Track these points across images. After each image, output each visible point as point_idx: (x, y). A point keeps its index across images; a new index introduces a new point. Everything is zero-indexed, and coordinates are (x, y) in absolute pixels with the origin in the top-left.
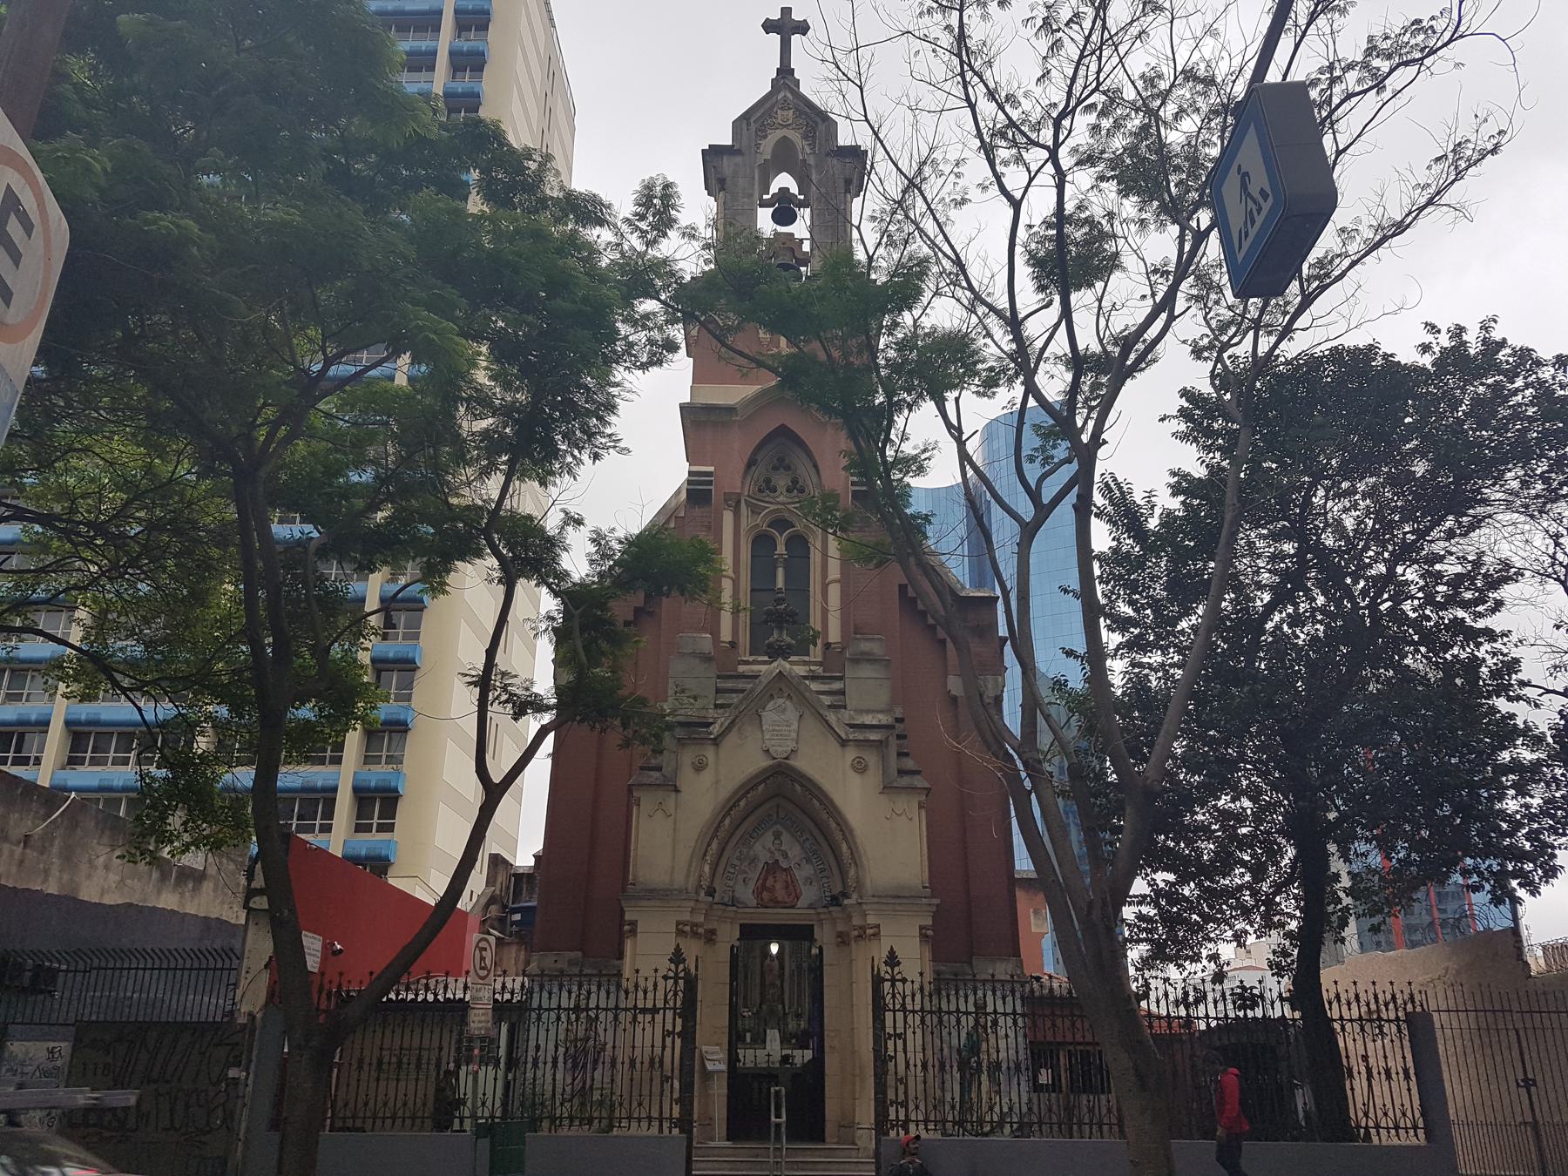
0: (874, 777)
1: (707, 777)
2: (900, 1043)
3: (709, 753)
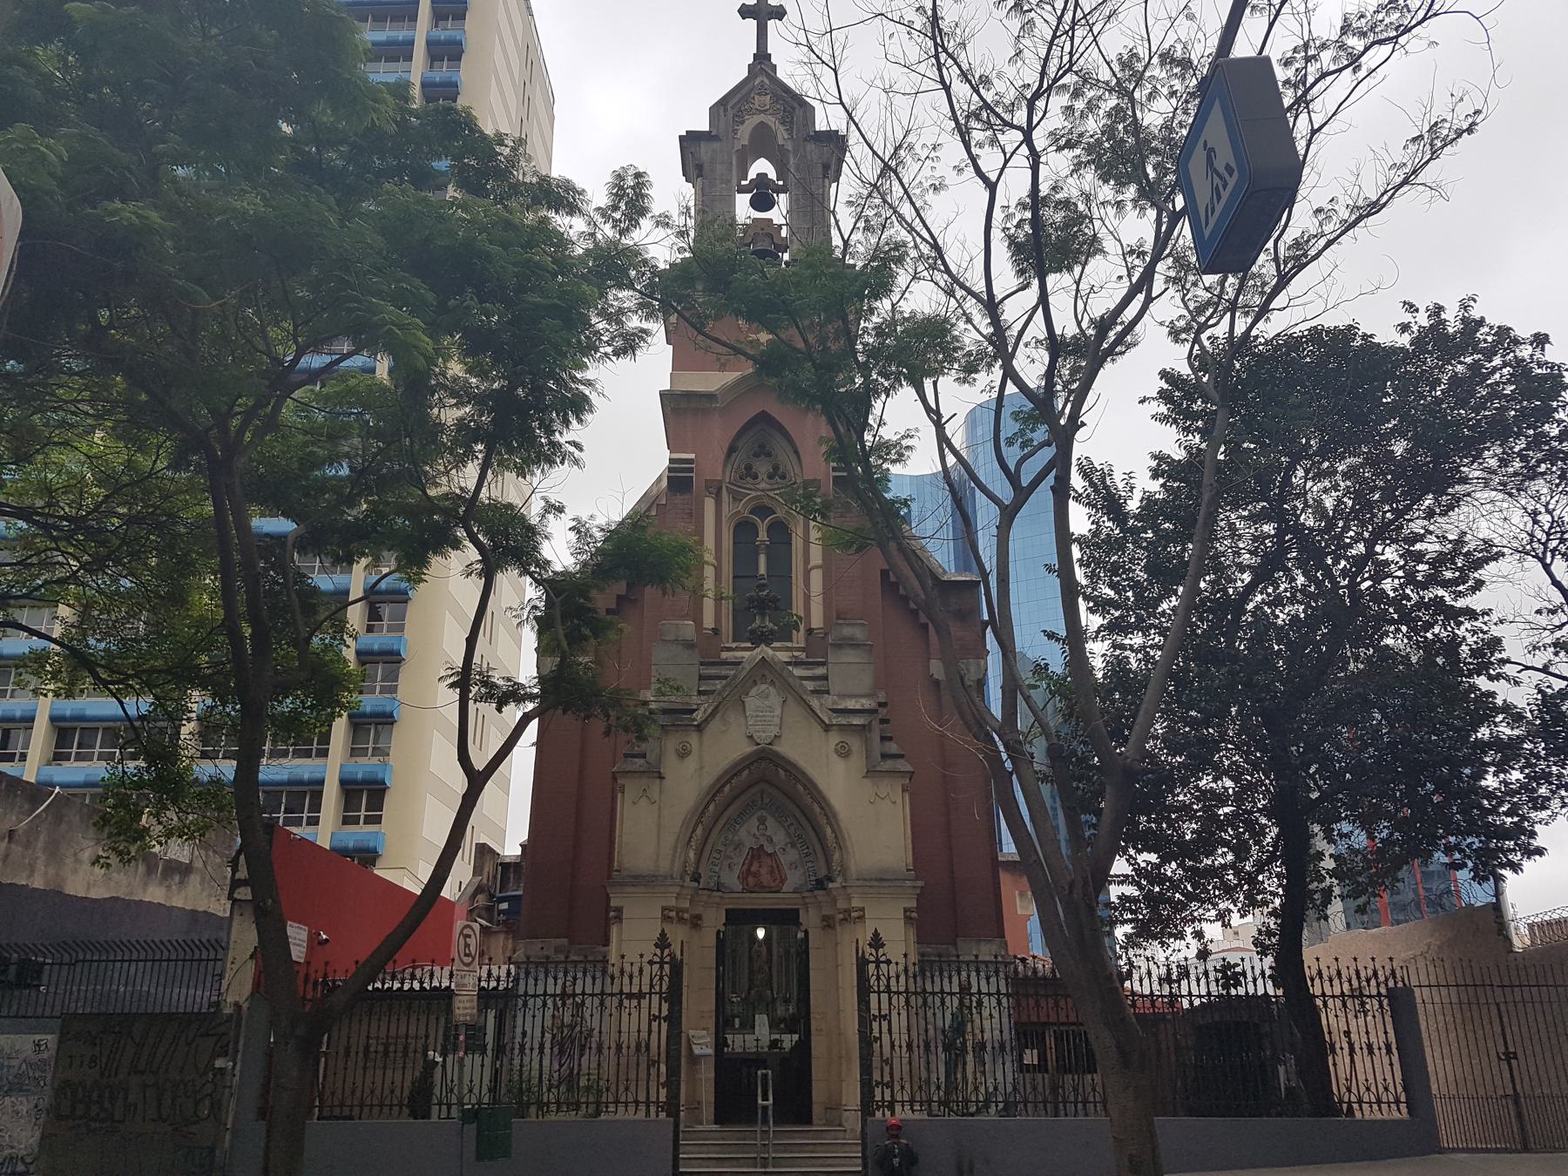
0: (857, 761)
1: (691, 763)
2: (885, 1024)
3: (693, 739)
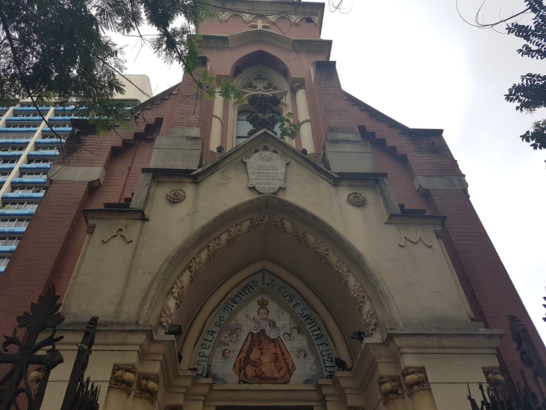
1: (183, 209)
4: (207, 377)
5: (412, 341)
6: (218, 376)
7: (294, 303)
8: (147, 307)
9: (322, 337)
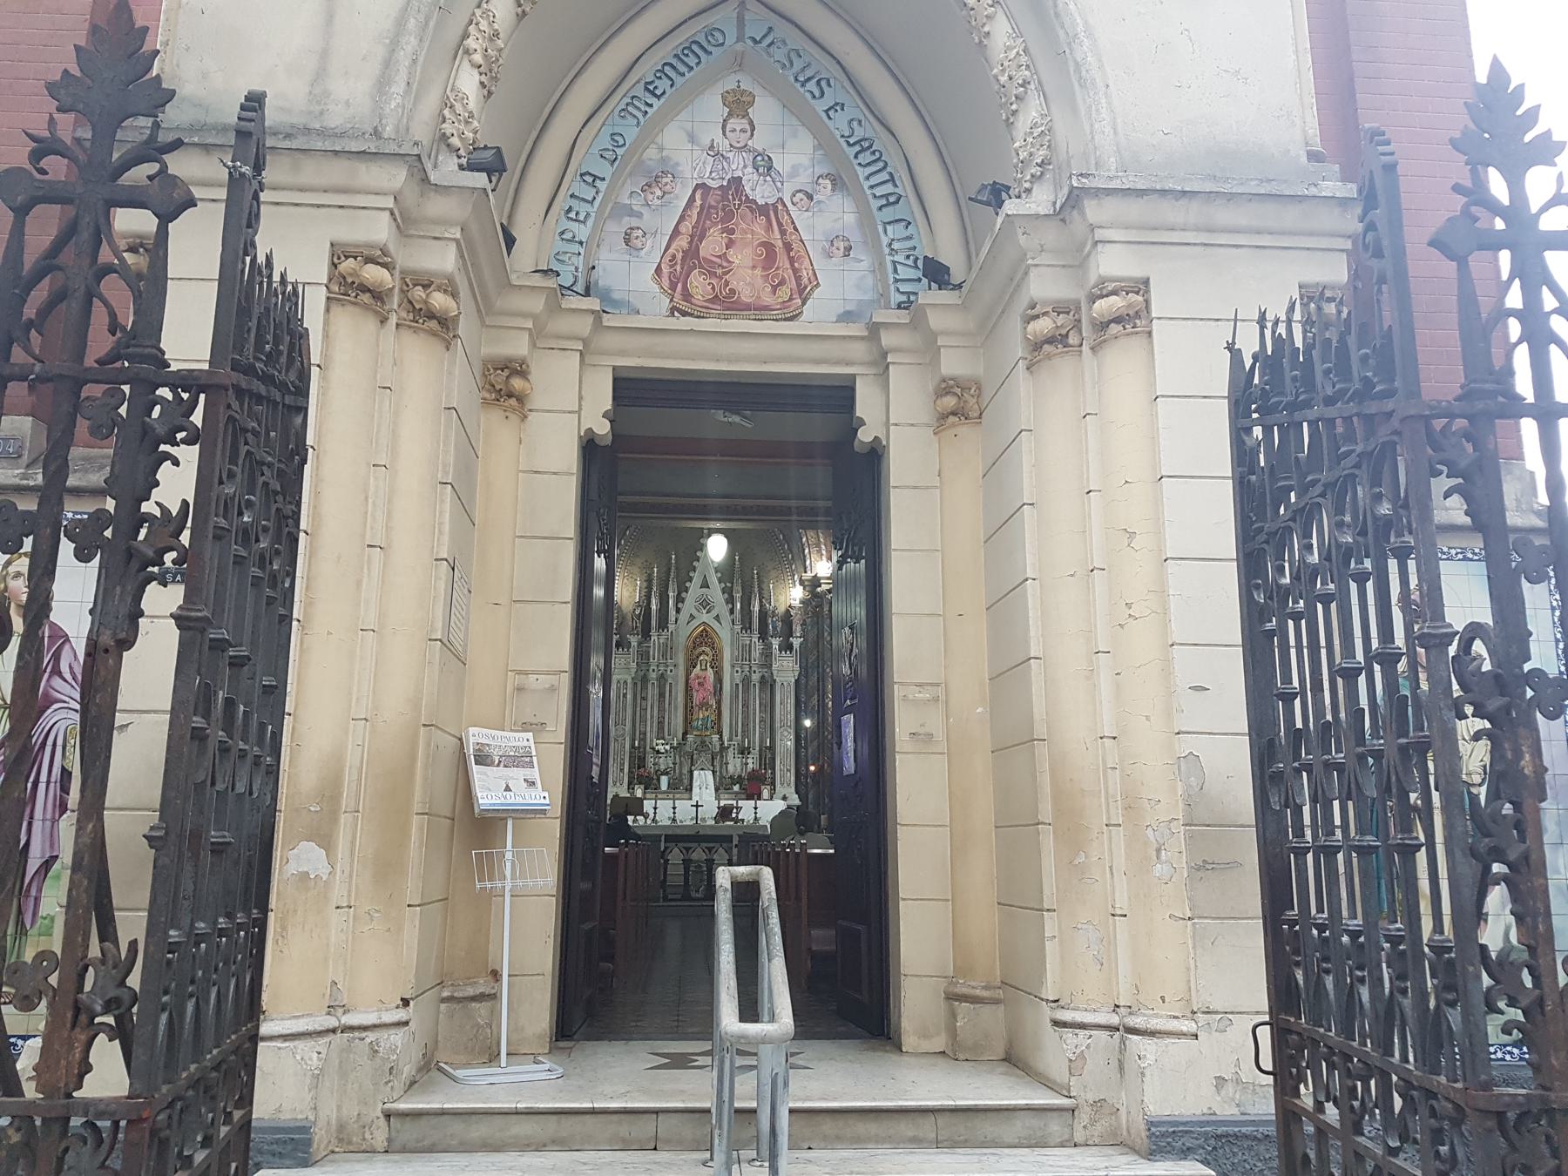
4: (587, 293)
5: (1134, 210)
6: (616, 296)
7: (828, 101)
8: (398, 88)
9: (897, 202)
